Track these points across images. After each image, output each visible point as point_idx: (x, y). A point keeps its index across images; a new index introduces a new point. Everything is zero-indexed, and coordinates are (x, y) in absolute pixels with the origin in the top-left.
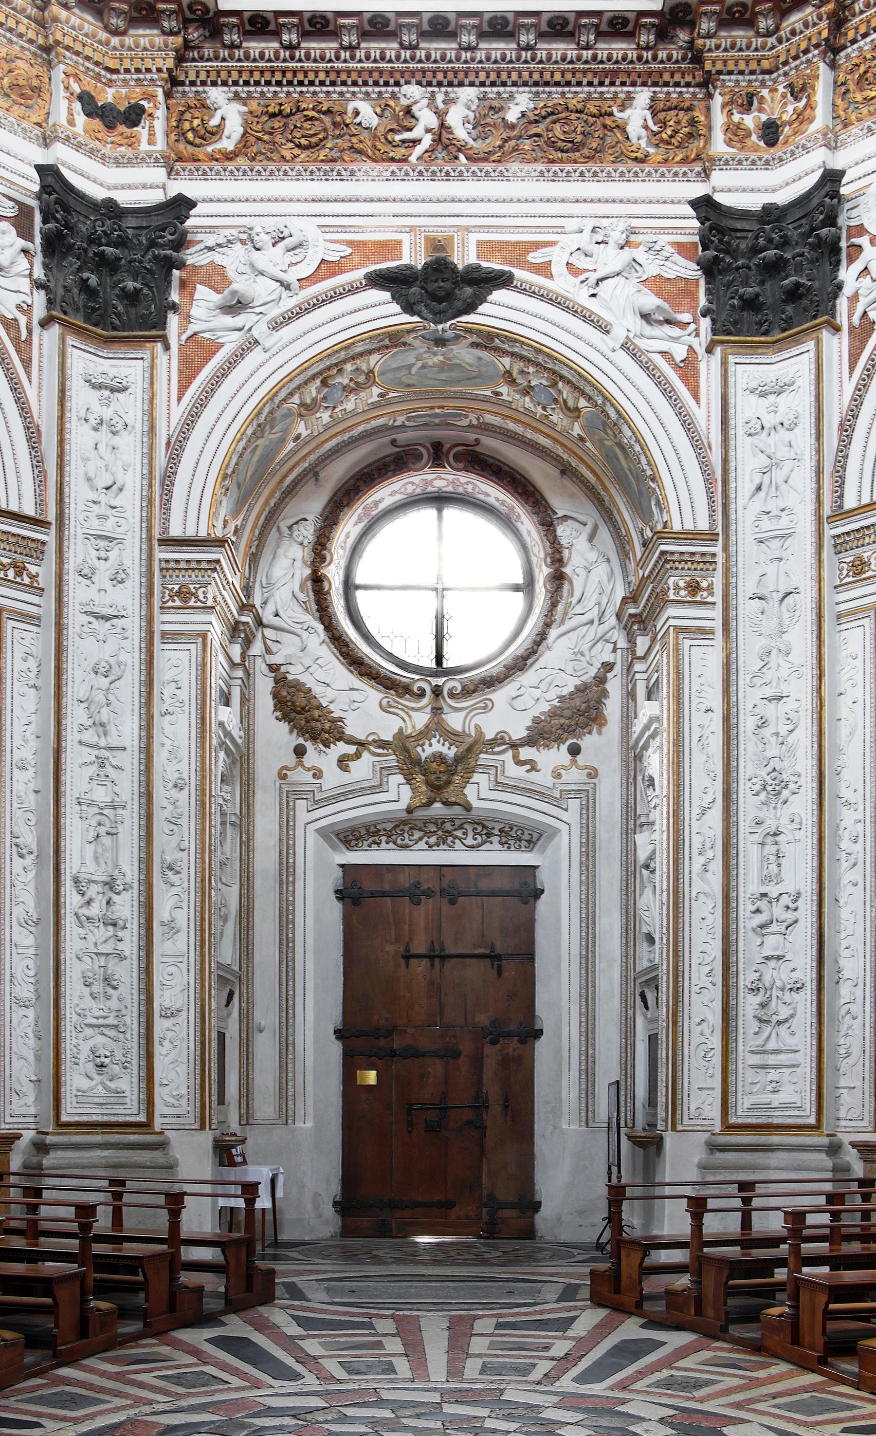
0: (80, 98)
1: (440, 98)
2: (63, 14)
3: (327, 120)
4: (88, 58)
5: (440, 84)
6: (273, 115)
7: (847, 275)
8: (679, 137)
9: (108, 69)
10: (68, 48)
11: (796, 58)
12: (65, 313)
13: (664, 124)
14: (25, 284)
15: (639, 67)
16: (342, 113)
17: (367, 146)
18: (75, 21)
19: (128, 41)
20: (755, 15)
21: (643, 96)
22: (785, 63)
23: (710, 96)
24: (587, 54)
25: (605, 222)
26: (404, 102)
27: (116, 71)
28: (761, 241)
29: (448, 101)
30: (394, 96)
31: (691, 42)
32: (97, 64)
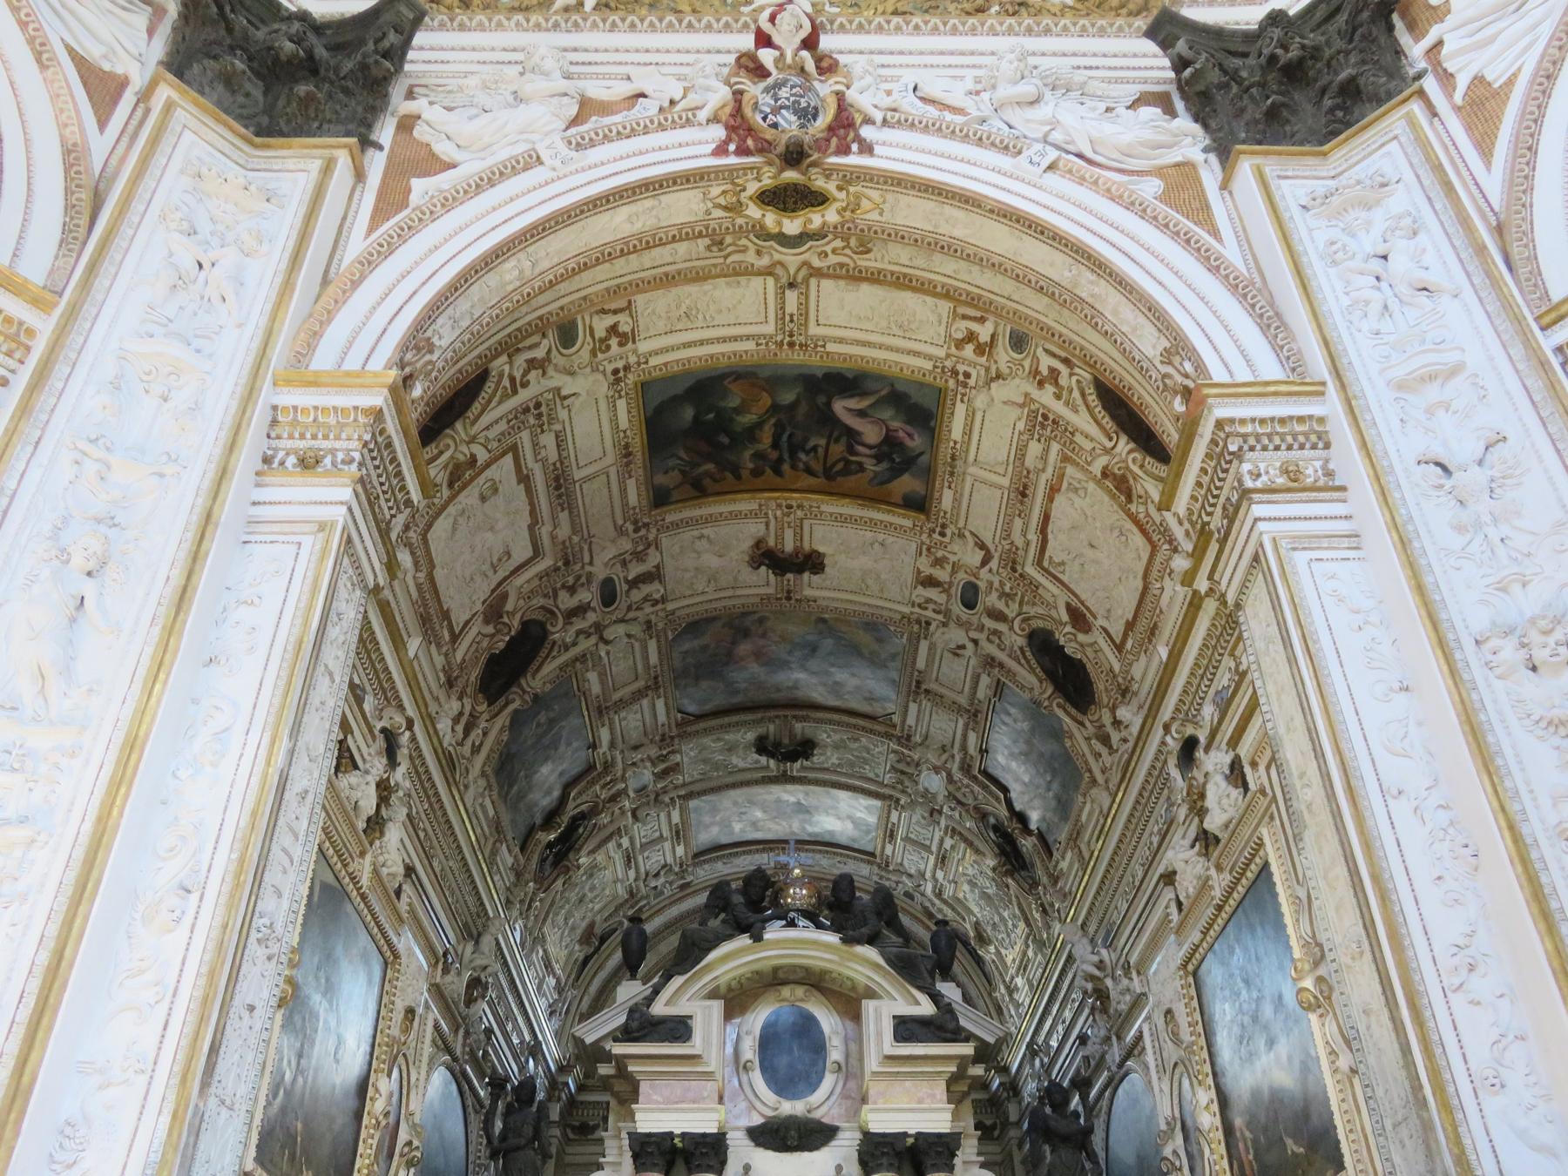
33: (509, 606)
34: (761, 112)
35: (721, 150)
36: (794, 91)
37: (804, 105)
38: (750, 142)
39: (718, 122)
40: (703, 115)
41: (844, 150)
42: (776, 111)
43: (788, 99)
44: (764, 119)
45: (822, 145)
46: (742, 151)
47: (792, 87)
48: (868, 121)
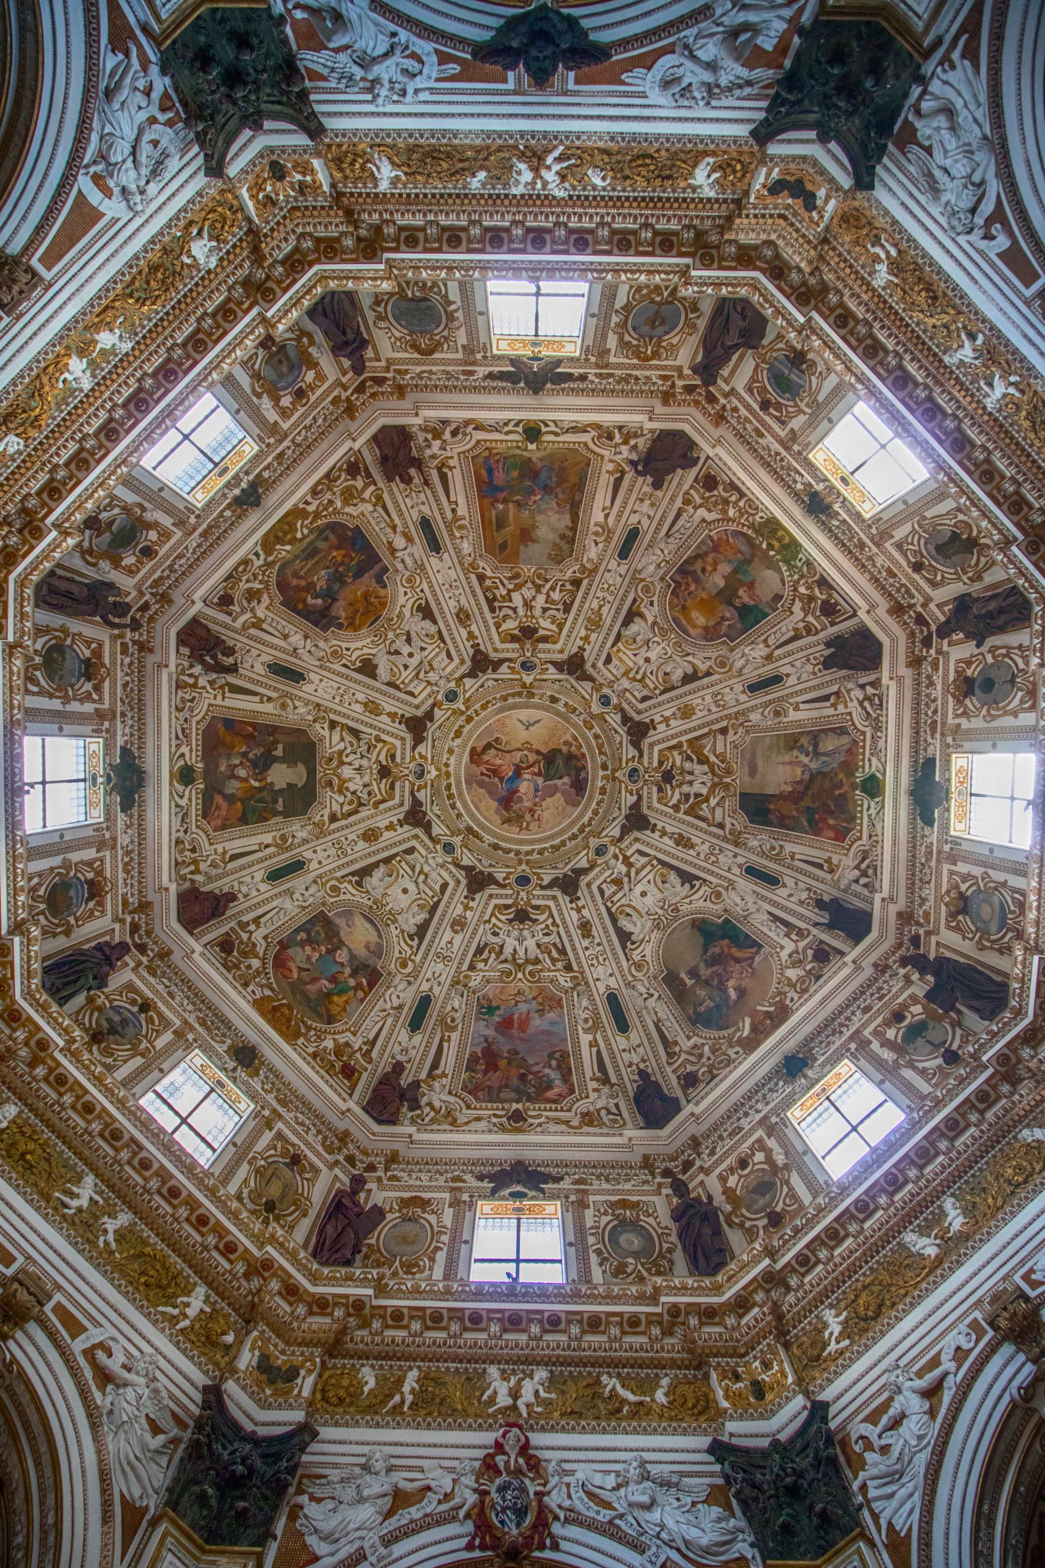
0: (815, 208)
1: (539, 186)
2: (803, 265)
3: (627, 172)
4: (797, 231)
5: (539, 196)
6: (669, 177)
7: (161, 84)
8: (348, 160)
9: (785, 218)
10: (809, 242)
11: (278, 223)
12: (911, 56)
13: (363, 168)
14: (935, 86)
15: (390, 207)
16: (614, 178)
17: (598, 157)
18: (797, 258)
19: (763, 237)
20: (317, 250)
21: (384, 186)
22: (284, 217)
23: (333, 186)
24: (431, 217)
25: (395, 98)
26: (567, 185)
27: (780, 216)
28: (253, 97)
29: (533, 183)
30: (574, 188)
31: (356, 228)
32: (792, 225)
35: (470, 1547)
40: (462, 1513)
41: (542, 1547)
42: (504, 1510)
46: (483, 1547)
48: (556, 1518)
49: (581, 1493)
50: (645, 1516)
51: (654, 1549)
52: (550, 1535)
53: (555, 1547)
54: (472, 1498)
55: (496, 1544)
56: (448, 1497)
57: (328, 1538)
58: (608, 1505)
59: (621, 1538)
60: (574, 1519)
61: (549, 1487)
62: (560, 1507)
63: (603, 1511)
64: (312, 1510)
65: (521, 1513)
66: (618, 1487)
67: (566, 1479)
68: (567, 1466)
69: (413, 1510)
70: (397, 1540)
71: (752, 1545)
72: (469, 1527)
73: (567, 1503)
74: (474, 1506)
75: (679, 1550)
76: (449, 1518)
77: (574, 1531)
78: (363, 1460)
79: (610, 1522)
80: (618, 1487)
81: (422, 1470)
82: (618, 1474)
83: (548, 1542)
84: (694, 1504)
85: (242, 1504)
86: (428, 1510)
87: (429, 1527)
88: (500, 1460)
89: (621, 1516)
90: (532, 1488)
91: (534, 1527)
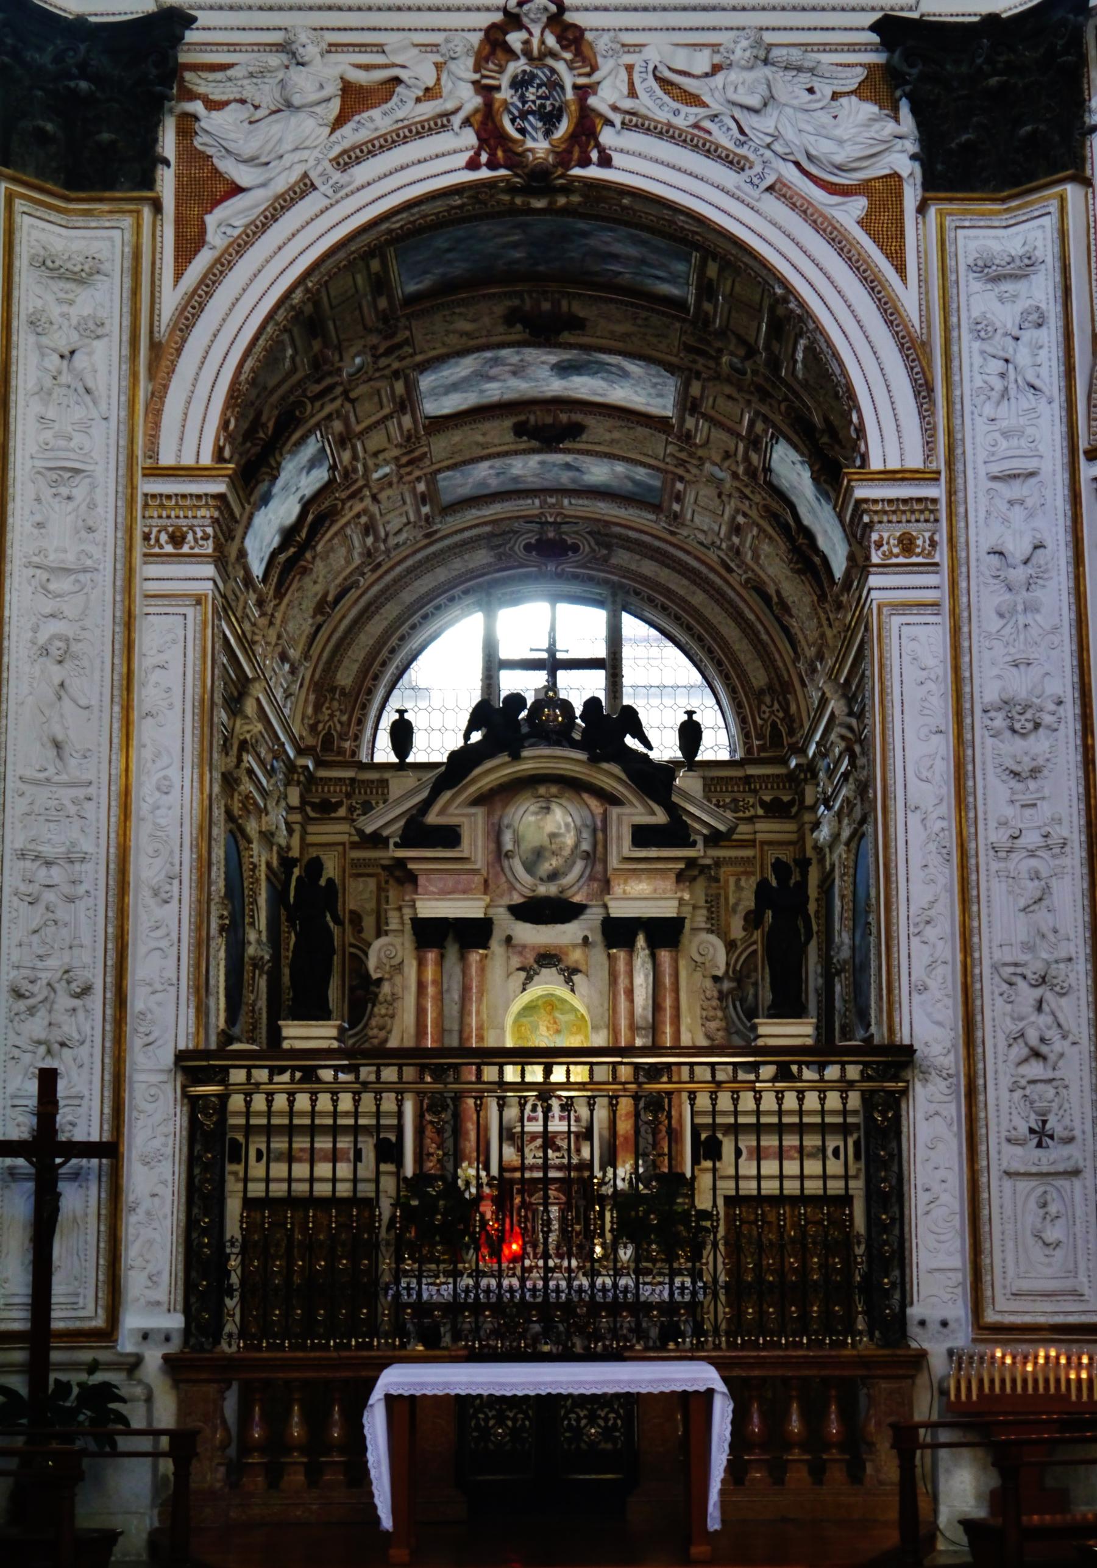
33: (264, 419)
34: (510, 112)
35: (473, 165)
36: (541, 91)
37: (549, 108)
38: (500, 154)
39: (471, 125)
40: (457, 120)
41: (585, 162)
42: (524, 115)
43: (534, 102)
44: (513, 121)
45: (564, 158)
46: (492, 165)
47: (539, 86)
48: (610, 123)
49: (652, 82)
50: (749, 121)
51: (758, 168)
52: (598, 145)
53: (606, 161)
54: (473, 101)
55: (515, 159)
56: (430, 93)
57: (250, 161)
58: (694, 100)
59: (711, 151)
60: (636, 122)
61: (596, 77)
62: (615, 108)
63: (685, 109)
64: (212, 121)
65: (550, 119)
66: (716, 69)
67: (628, 59)
68: (628, 38)
69: (375, 113)
70: (358, 161)
71: (913, 157)
72: (470, 138)
73: (627, 104)
74: (476, 111)
75: (797, 164)
76: (440, 123)
77: (635, 140)
78: (277, 37)
79: (696, 126)
80: (716, 69)
81: (380, 48)
82: (715, 47)
83: (594, 155)
84: (835, 96)
85: (106, 136)
86: (400, 114)
87: (405, 140)
88: (515, 39)
89: (713, 118)
90: (568, 80)
91: (573, 137)
